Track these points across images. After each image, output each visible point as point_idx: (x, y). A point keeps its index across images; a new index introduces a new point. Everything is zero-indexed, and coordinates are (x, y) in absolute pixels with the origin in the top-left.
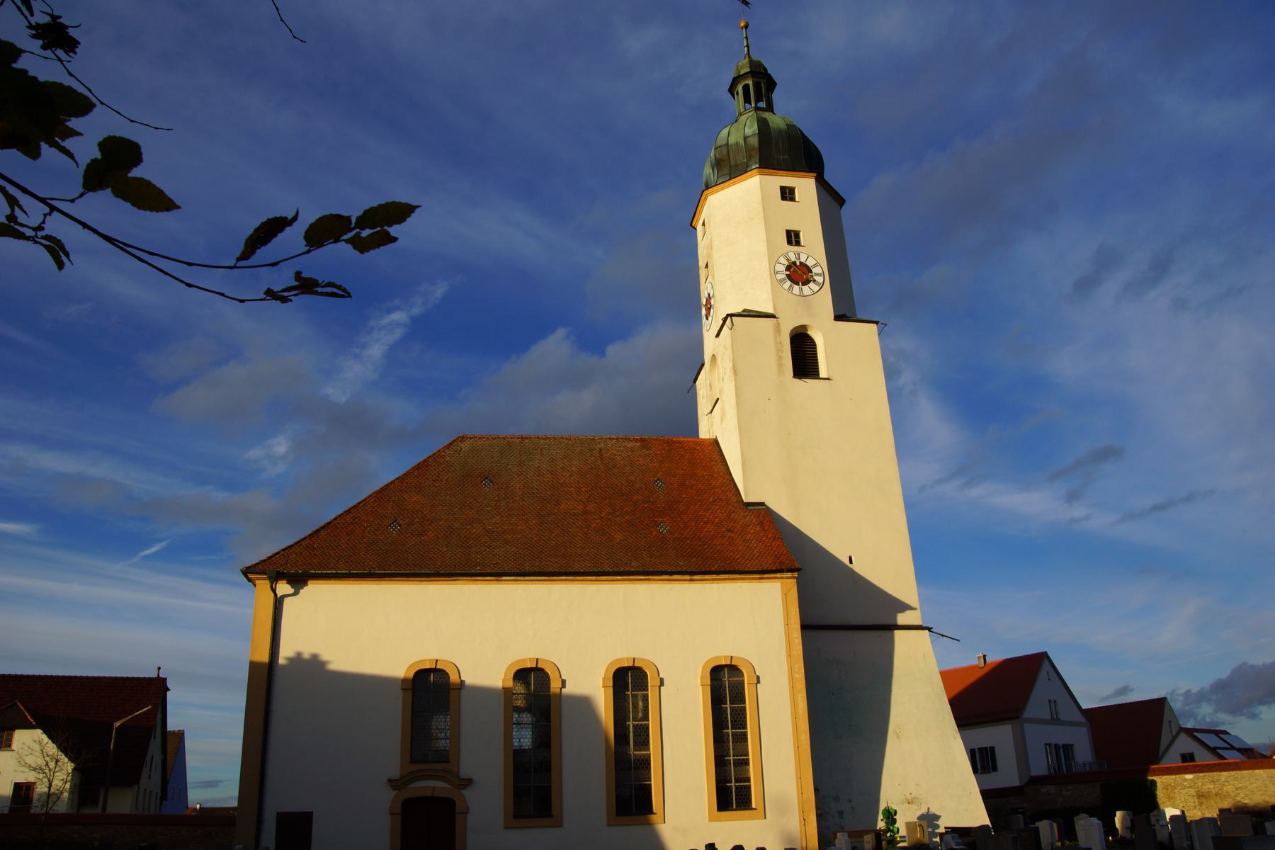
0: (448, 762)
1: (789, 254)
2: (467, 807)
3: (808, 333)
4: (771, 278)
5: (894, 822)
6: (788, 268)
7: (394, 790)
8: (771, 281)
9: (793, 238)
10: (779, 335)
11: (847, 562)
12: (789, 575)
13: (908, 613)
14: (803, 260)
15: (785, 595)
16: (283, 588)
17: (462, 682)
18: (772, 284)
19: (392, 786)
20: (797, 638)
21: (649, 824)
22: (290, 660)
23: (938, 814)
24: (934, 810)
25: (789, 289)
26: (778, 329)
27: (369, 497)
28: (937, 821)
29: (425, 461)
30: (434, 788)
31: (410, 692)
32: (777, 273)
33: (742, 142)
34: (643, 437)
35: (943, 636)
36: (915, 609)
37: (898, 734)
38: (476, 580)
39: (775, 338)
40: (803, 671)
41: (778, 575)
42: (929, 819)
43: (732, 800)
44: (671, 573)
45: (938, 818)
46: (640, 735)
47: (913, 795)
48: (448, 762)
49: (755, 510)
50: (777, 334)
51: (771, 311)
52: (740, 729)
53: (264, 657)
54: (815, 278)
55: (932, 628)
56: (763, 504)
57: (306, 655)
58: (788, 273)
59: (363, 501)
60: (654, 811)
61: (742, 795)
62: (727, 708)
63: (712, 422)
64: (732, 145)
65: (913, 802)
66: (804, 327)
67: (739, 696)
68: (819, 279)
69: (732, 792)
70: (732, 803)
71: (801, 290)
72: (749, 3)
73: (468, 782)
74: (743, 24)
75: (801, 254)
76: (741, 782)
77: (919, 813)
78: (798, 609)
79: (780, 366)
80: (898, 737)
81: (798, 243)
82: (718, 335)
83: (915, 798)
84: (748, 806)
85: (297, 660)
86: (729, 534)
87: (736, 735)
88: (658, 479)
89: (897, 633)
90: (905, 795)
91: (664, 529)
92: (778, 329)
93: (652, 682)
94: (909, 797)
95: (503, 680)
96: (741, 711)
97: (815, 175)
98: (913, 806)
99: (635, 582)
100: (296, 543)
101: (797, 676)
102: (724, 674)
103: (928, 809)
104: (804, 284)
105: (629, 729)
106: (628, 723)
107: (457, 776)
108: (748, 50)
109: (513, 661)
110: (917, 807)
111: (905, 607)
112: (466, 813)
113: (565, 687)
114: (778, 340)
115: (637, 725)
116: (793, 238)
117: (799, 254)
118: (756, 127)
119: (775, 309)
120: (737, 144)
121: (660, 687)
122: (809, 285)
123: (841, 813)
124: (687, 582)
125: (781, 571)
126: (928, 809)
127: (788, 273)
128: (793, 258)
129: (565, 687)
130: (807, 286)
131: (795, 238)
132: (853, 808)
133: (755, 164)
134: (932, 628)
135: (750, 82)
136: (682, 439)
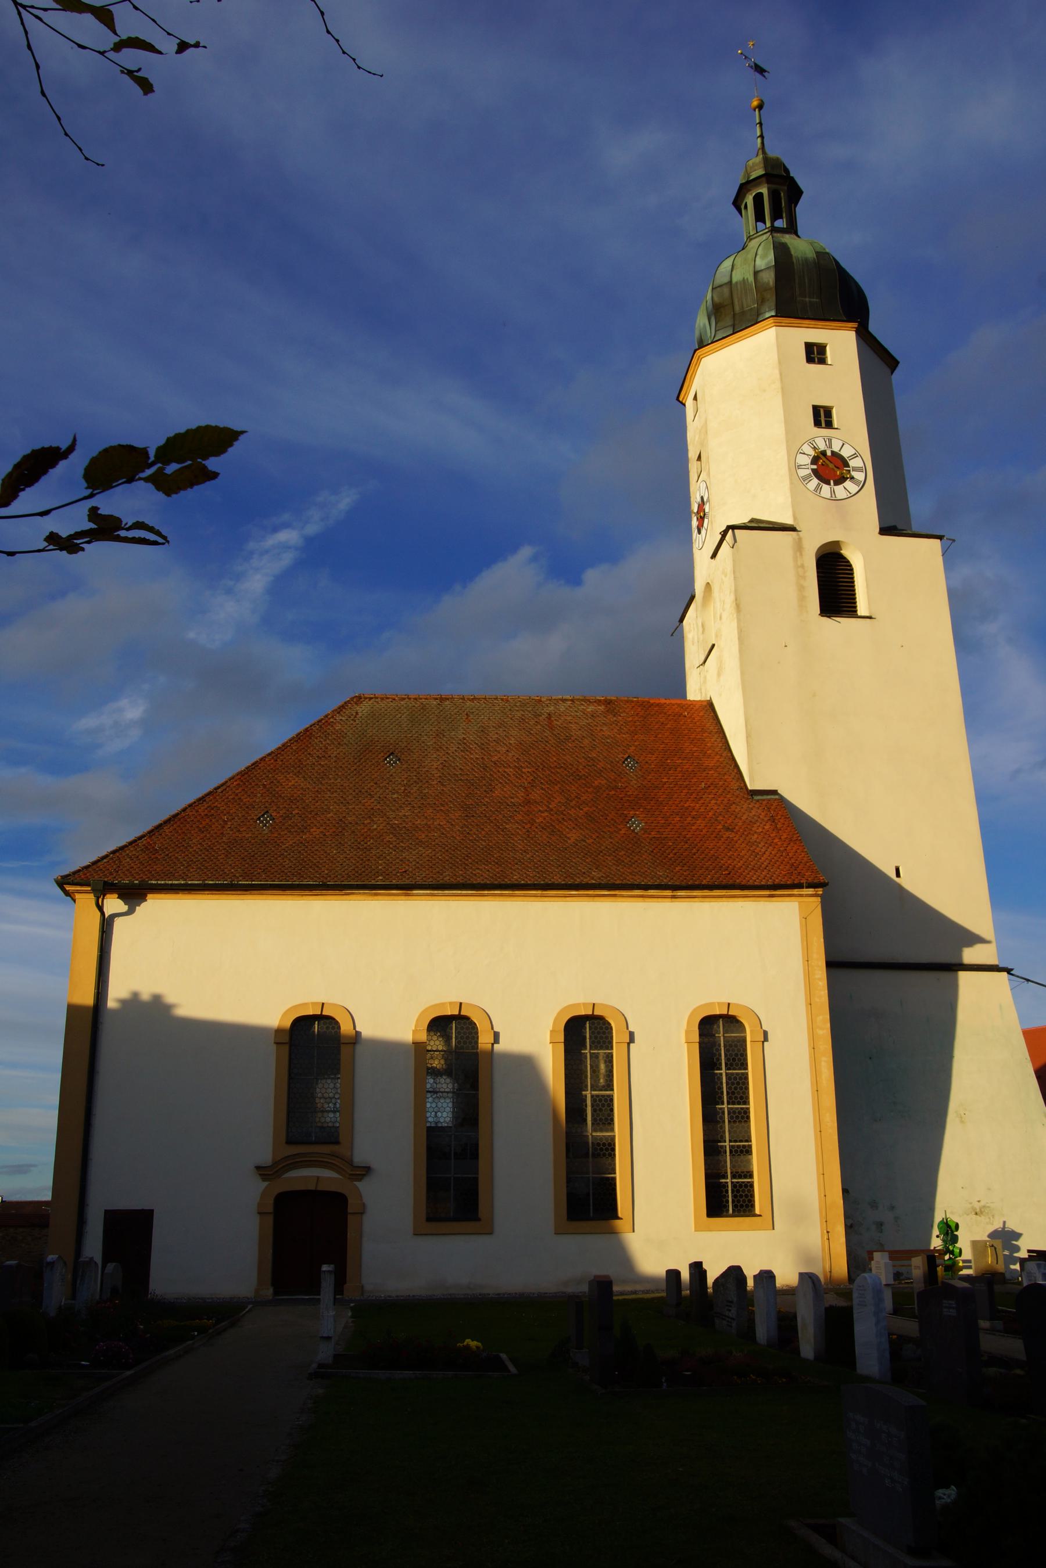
0: (337, 1143)
1: (816, 440)
2: (364, 1205)
3: (842, 552)
4: (791, 475)
5: (955, 1239)
6: (815, 460)
7: (264, 1180)
8: (791, 479)
9: (822, 417)
10: (801, 555)
11: (892, 874)
12: (811, 891)
13: (979, 947)
14: (836, 449)
15: (805, 919)
16: (113, 904)
17: (358, 1034)
18: (791, 483)
19: (260, 1175)
20: (820, 979)
21: (613, 1232)
22: (124, 1002)
23: (1018, 1230)
24: (1012, 1225)
25: (816, 490)
26: (799, 547)
27: (230, 779)
28: (1017, 1240)
29: (307, 730)
30: (318, 1178)
31: (287, 1047)
32: (799, 467)
33: (751, 279)
34: (608, 698)
35: (1028, 980)
36: (989, 942)
37: (961, 1117)
38: (376, 895)
39: (795, 560)
40: (828, 1025)
41: (796, 892)
42: (1006, 1237)
43: (728, 1201)
44: (646, 888)
45: (1017, 1236)
46: (601, 1110)
47: (982, 1203)
48: (337, 1143)
49: (764, 800)
50: (798, 554)
51: (788, 521)
52: (739, 1103)
53: (86, 997)
54: (853, 474)
55: (1012, 970)
56: (774, 792)
57: (145, 996)
58: (815, 467)
59: (223, 785)
60: (620, 1215)
61: (741, 1196)
62: (721, 1074)
63: (705, 677)
64: (736, 283)
65: (981, 1212)
66: (837, 544)
67: (738, 1058)
68: (859, 476)
69: (727, 1191)
70: (727, 1207)
71: (833, 492)
72: (765, 71)
73: (365, 1171)
74: (755, 103)
75: (834, 441)
76: (740, 1177)
77: (991, 1229)
78: (822, 940)
79: (802, 599)
80: (962, 1122)
81: (829, 425)
82: (714, 556)
83: (984, 1207)
84: (750, 1211)
85: (133, 1003)
86: (727, 834)
87: (734, 1112)
88: (629, 756)
89: (963, 975)
90: (971, 1203)
91: (637, 825)
92: (799, 547)
93: (618, 1037)
94: (977, 1206)
95: (414, 1032)
96: (740, 1078)
97: (855, 325)
98: (982, 1219)
99: (596, 898)
100: (131, 843)
101: (820, 1032)
102: (719, 1027)
103: (1004, 1223)
104: (837, 483)
105: (585, 1101)
106: (584, 1093)
107: (350, 1162)
108: (763, 143)
109: (427, 1006)
110: (988, 1220)
112: (362, 1213)
113: (498, 1043)
114: (799, 564)
115: (597, 1096)
116: (822, 417)
117: (830, 441)
118: (771, 256)
119: (795, 518)
120: (744, 281)
121: (629, 1044)
122: (844, 484)
123: (880, 1225)
124: (669, 900)
125: (800, 886)
126: (1004, 1223)
127: (815, 467)
128: (822, 446)
129: (498, 1043)
130: (842, 485)
131: (825, 417)
133: (770, 310)
134: (1012, 970)
135: (764, 190)
136: (663, 701)
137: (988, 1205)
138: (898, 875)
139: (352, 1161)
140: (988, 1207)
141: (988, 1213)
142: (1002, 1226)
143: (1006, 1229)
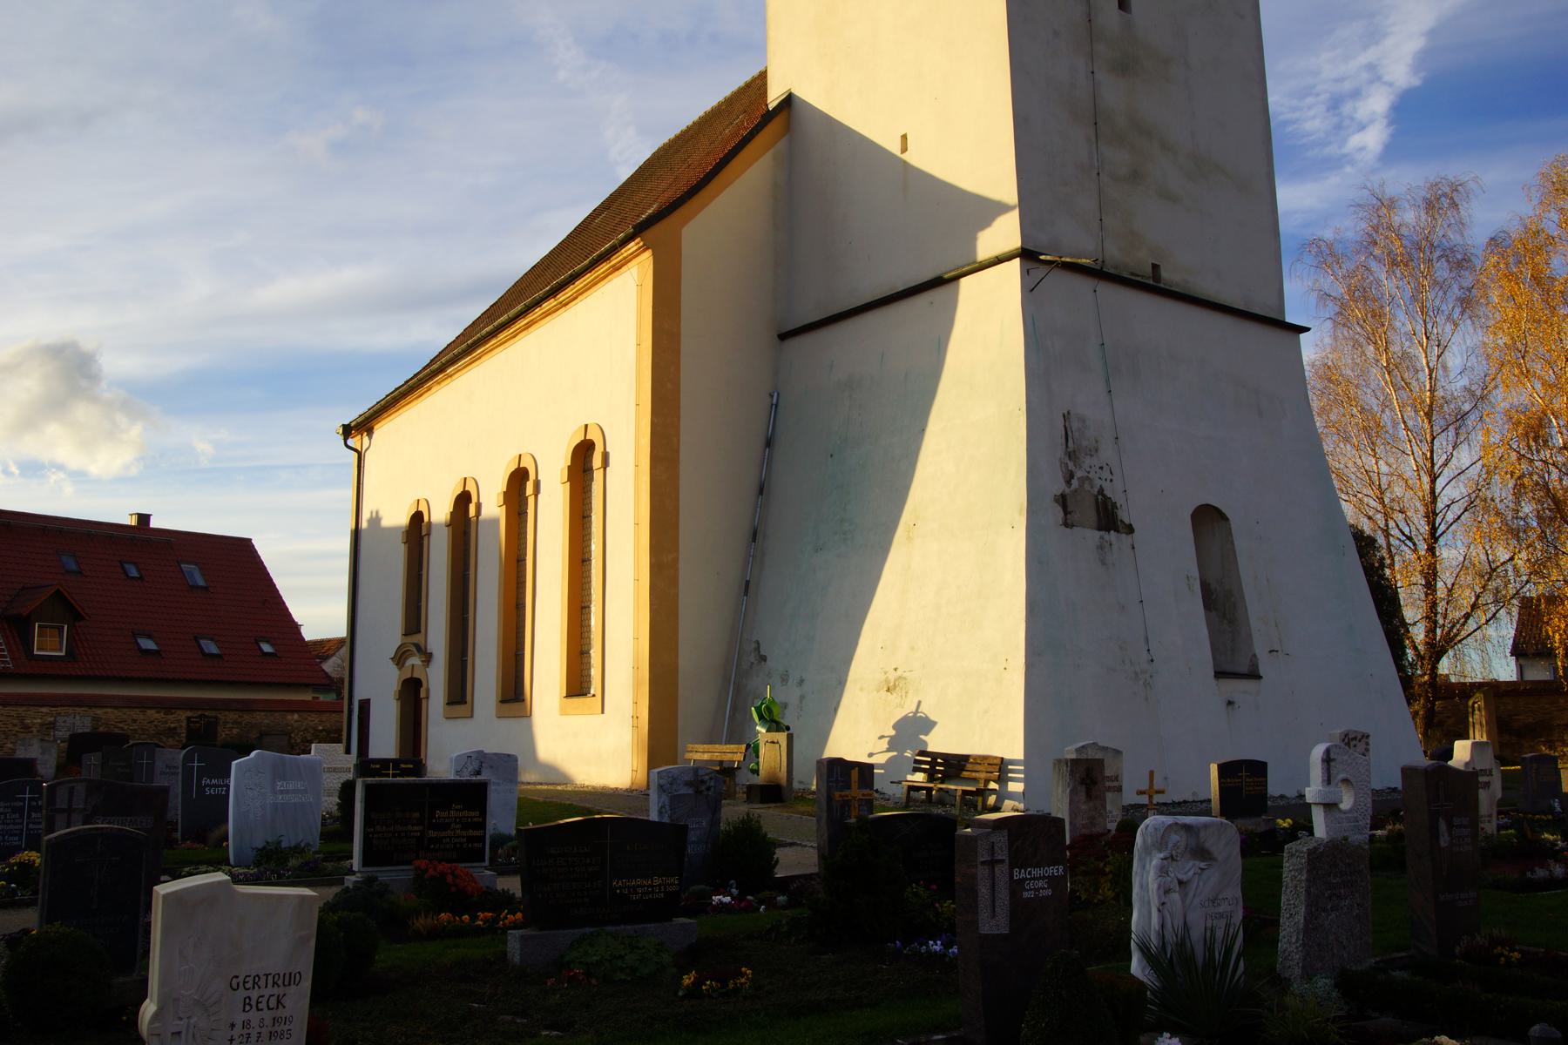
12: (632, 247)
23: (932, 718)
24: (926, 710)
28: (927, 734)
42: (913, 726)
45: (927, 725)
47: (899, 673)
94: (892, 676)
98: (892, 697)
103: (919, 703)
111: (988, 211)
126: (919, 703)
132: (802, 698)
137: (905, 675)
138: (904, 149)
139: (426, 648)
140: (905, 678)
141: (901, 689)
142: (913, 708)
143: (919, 715)
